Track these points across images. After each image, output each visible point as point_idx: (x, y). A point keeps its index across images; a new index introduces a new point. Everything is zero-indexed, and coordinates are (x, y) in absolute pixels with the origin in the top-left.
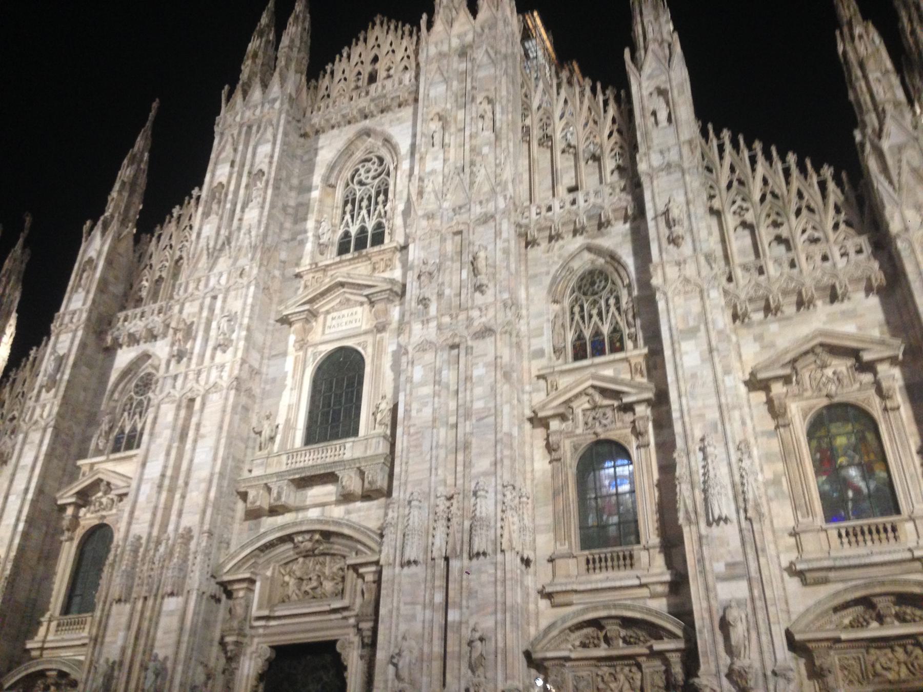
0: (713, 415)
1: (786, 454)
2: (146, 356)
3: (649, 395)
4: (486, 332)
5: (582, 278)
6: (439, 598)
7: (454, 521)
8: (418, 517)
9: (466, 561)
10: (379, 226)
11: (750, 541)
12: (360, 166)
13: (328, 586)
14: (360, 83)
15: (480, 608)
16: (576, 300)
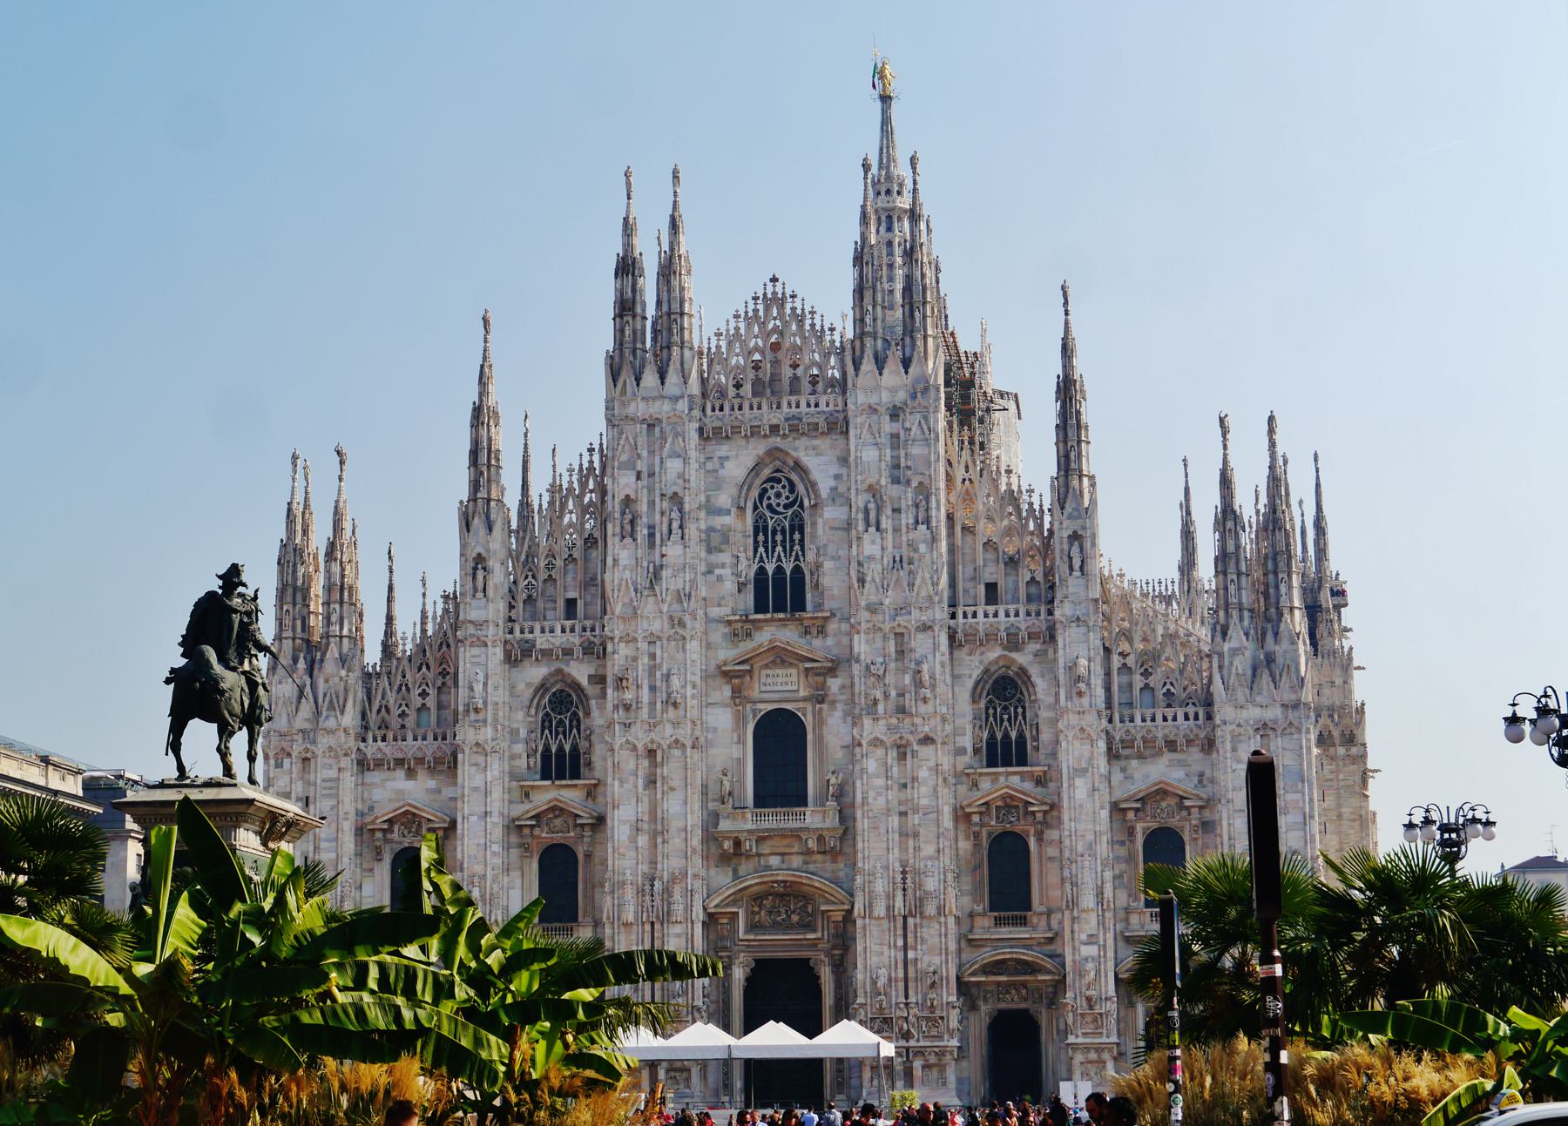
0: (1090, 837)
1: (1130, 859)
2: (559, 671)
3: (1045, 808)
4: (927, 740)
5: (996, 682)
6: (900, 942)
7: (910, 891)
8: (880, 886)
9: (918, 920)
10: (797, 570)
11: (1101, 923)
12: (768, 485)
13: (795, 918)
14: (761, 375)
15: (930, 951)
16: (991, 701)
